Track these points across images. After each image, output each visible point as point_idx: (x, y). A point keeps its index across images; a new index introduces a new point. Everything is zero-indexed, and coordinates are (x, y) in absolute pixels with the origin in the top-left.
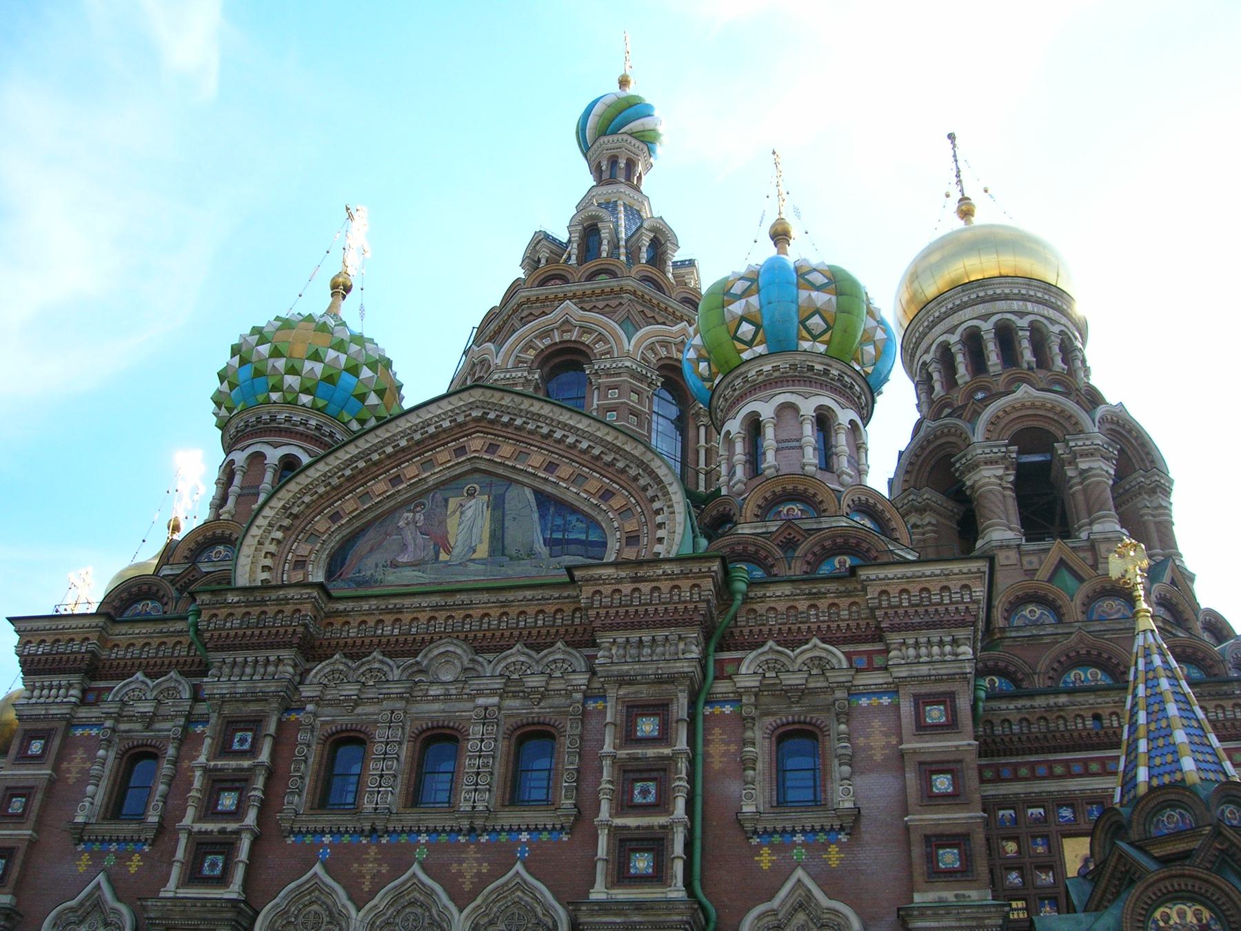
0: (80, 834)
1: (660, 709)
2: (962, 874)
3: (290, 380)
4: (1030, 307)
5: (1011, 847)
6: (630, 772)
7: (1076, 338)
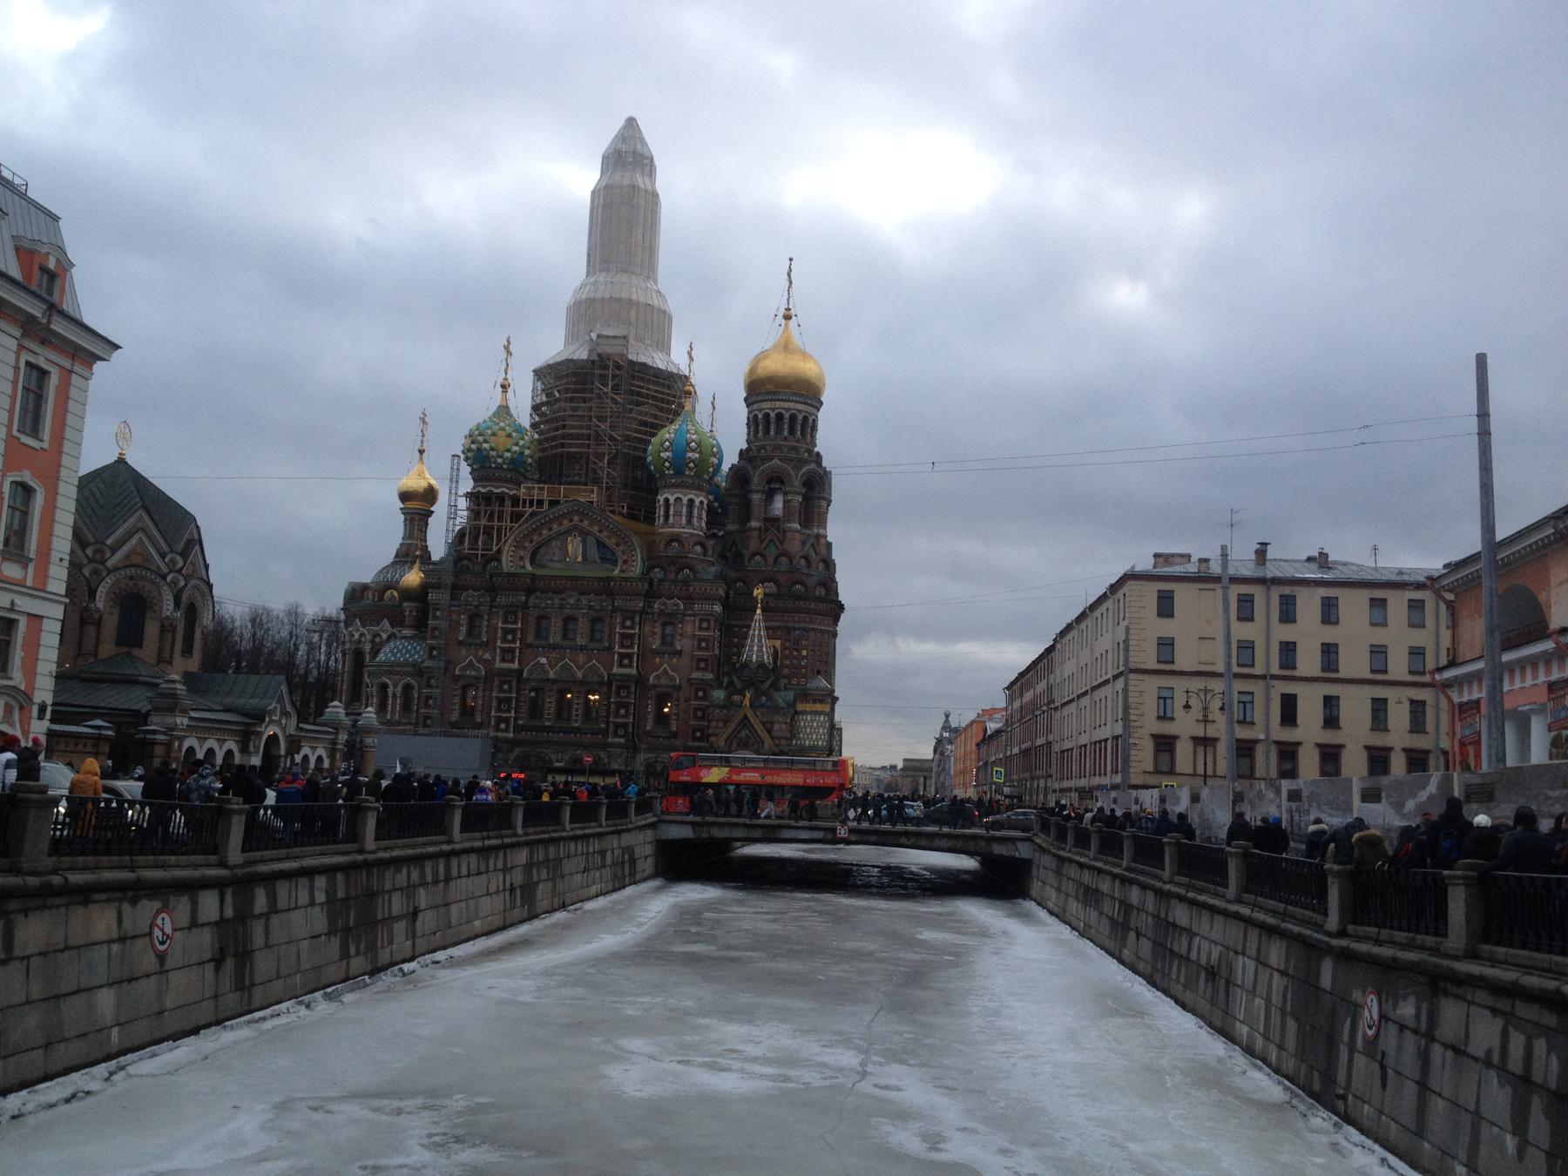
0: (461, 643)
1: (632, 619)
2: (705, 669)
3: (499, 460)
4: (792, 405)
5: (736, 640)
6: (623, 636)
7: (811, 414)
